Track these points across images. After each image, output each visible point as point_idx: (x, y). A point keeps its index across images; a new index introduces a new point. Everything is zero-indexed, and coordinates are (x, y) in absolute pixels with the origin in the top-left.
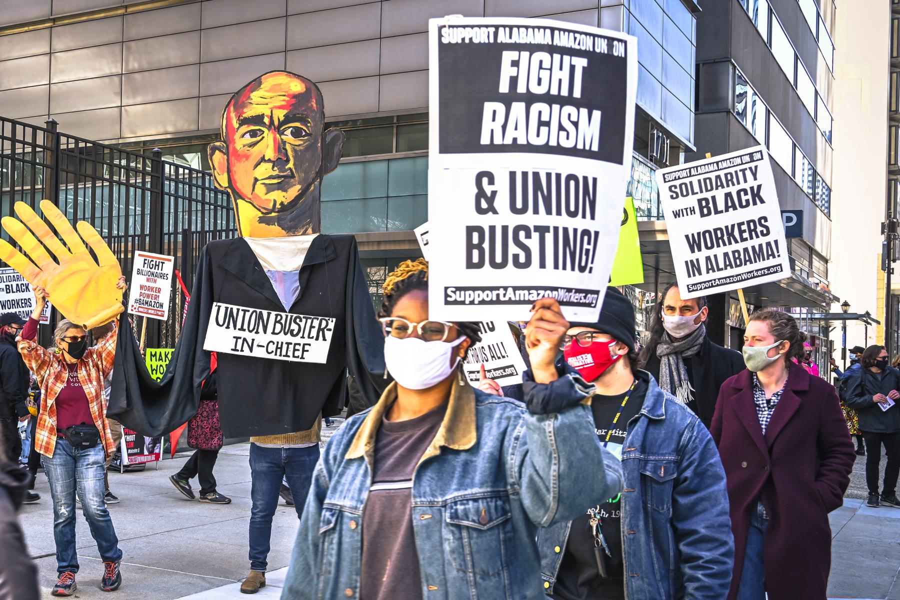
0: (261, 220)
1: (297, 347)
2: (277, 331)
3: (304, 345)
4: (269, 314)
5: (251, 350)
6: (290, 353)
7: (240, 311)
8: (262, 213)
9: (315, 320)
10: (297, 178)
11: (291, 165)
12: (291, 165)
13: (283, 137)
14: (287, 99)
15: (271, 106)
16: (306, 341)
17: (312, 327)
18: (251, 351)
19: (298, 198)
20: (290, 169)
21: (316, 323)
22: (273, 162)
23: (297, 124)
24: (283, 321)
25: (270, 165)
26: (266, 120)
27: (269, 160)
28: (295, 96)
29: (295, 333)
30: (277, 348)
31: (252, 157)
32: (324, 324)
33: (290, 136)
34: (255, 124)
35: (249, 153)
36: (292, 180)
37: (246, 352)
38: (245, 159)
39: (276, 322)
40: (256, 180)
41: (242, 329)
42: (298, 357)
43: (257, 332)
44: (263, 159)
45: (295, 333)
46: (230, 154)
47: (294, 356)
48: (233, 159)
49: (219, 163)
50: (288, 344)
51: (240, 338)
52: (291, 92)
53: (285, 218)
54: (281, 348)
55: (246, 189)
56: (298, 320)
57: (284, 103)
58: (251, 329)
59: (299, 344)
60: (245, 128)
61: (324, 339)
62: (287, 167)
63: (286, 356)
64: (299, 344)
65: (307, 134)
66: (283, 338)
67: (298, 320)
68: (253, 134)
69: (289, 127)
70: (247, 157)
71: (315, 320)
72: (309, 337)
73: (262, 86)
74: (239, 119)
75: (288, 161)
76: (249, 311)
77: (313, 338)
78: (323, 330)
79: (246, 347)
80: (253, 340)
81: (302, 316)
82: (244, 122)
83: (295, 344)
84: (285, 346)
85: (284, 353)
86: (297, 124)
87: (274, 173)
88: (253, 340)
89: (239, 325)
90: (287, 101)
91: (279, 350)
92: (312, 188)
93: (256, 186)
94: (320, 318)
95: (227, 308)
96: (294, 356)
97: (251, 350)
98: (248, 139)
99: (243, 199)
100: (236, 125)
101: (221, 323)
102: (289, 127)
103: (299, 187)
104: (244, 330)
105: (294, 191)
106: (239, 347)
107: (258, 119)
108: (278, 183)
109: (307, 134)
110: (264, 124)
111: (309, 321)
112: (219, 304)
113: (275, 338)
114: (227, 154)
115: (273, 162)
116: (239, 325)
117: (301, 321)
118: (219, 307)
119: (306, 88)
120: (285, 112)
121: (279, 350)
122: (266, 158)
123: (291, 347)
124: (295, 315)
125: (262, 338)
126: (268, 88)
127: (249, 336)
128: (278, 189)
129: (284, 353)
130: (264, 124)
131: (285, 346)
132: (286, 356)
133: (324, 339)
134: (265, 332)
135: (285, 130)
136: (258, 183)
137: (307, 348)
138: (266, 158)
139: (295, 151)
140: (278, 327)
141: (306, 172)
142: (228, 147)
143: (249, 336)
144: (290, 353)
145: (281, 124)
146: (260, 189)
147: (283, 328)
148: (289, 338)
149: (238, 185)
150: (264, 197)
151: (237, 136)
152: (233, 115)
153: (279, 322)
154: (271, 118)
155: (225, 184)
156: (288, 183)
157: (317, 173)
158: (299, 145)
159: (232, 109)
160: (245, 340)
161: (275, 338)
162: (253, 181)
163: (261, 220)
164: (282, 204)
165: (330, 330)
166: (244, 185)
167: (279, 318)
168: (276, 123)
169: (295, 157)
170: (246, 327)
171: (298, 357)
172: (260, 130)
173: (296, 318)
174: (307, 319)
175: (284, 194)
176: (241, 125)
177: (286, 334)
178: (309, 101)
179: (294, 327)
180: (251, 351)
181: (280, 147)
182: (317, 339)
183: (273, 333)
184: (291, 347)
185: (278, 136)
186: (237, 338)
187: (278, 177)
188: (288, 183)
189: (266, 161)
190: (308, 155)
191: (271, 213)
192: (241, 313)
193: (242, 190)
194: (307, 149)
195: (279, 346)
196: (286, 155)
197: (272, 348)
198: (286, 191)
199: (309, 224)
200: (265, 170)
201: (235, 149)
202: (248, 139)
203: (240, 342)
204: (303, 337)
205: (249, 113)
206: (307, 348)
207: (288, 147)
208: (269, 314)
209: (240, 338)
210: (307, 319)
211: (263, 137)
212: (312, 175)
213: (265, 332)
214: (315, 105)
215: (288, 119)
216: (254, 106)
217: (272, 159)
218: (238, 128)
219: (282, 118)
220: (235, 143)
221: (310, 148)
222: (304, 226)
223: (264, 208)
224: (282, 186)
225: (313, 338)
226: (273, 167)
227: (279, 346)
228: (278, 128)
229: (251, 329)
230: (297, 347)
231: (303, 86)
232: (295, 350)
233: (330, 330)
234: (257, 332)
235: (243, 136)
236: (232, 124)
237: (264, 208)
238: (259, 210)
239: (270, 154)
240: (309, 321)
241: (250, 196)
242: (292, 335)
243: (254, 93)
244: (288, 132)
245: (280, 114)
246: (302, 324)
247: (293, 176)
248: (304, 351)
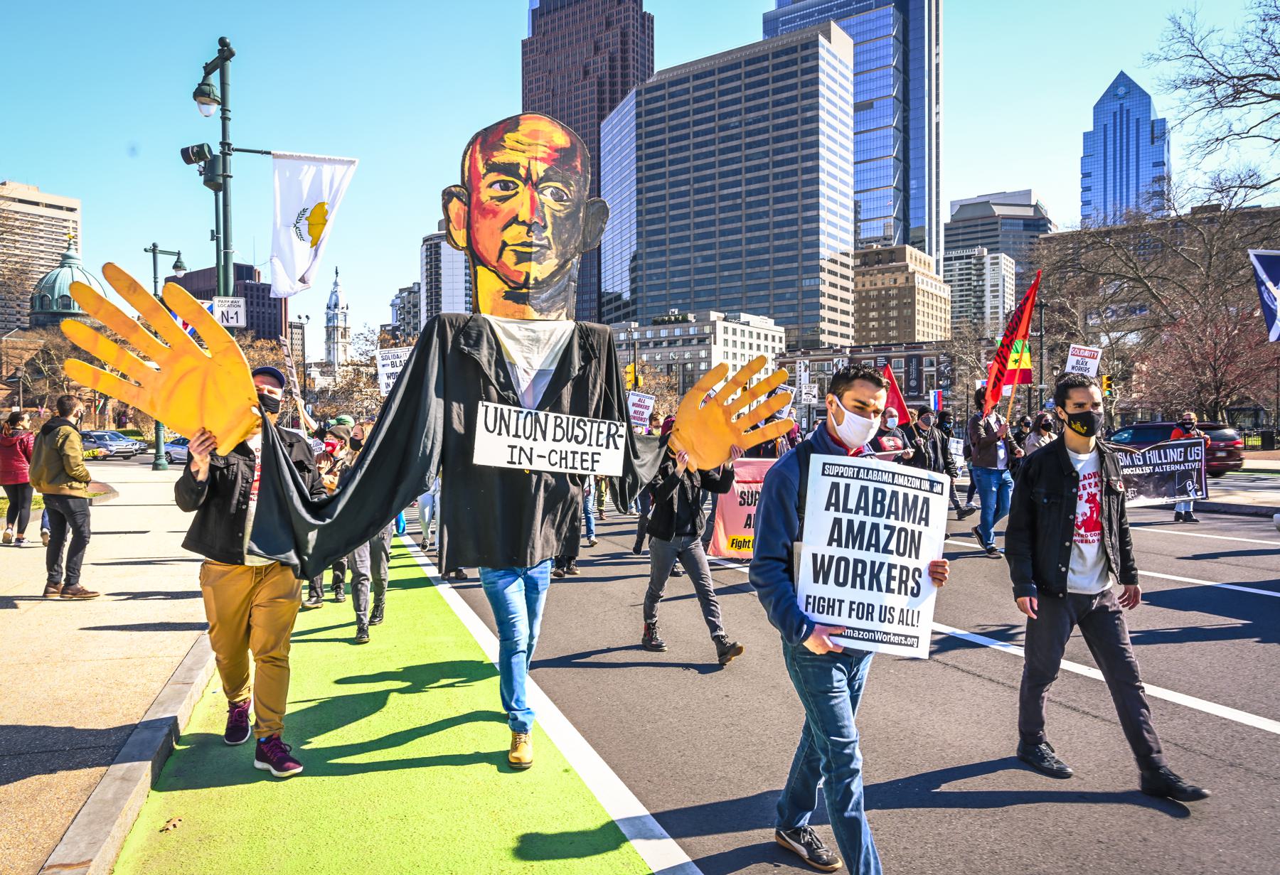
0: (507, 296)
1: (585, 457)
2: (558, 437)
3: (593, 454)
4: (547, 416)
5: (530, 461)
6: (578, 464)
7: (512, 412)
8: (510, 287)
9: (602, 425)
11: (548, 233)
12: (548, 233)
13: (541, 196)
14: (548, 151)
16: (595, 449)
17: (599, 433)
18: (531, 463)
19: (553, 275)
20: (547, 238)
21: (604, 428)
23: (559, 185)
24: (564, 425)
25: (524, 229)
26: (522, 172)
27: (524, 223)
28: (556, 150)
29: (580, 439)
30: (561, 459)
31: (501, 216)
32: (613, 430)
33: (550, 198)
34: (507, 175)
35: (497, 209)
36: (549, 252)
37: (525, 465)
38: (491, 215)
39: (556, 426)
41: (516, 436)
42: (587, 469)
43: (535, 439)
44: (515, 220)
45: (580, 439)
46: (472, 206)
47: (583, 468)
48: (476, 214)
49: (458, 215)
50: (574, 453)
51: (515, 447)
52: (553, 144)
53: (539, 298)
54: (566, 458)
55: (490, 253)
56: (582, 424)
57: (544, 155)
58: (527, 435)
59: (587, 454)
60: (493, 177)
61: (616, 448)
62: (544, 235)
63: (573, 468)
64: (587, 454)
66: (566, 446)
67: (582, 424)
68: (505, 185)
69: (549, 187)
70: (495, 213)
71: (602, 425)
72: (597, 445)
73: (520, 128)
74: (486, 164)
75: (545, 227)
76: (522, 412)
77: (602, 445)
78: (613, 436)
79: (524, 459)
80: (532, 449)
81: (586, 419)
82: (492, 168)
83: (582, 453)
84: (570, 456)
85: (570, 464)
86: (559, 185)
88: (532, 449)
89: (512, 431)
90: (549, 155)
91: (563, 461)
93: (505, 253)
94: (608, 422)
95: (496, 409)
96: (583, 468)
97: (530, 461)
98: (497, 191)
99: (486, 266)
100: (482, 170)
101: (491, 429)
102: (549, 187)
103: (556, 261)
104: (520, 437)
106: (516, 459)
107: (511, 169)
110: (519, 177)
111: (595, 425)
112: (486, 403)
113: (557, 446)
116: (512, 431)
117: (585, 425)
118: (487, 407)
119: (571, 143)
120: (546, 166)
121: (563, 461)
122: (520, 219)
123: (578, 457)
124: (577, 418)
125: (542, 447)
126: (526, 132)
127: (527, 445)
129: (570, 464)
130: (519, 177)
131: (570, 456)
132: (573, 468)
133: (616, 448)
134: (544, 439)
135: (544, 188)
136: (507, 248)
137: (596, 457)
138: (520, 219)
139: (554, 216)
140: (559, 431)
141: (565, 245)
142: (470, 196)
143: (527, 445)
144: (578, 464)
146: (509, 258)
147: (565, 434)
148: (573, 446)
149: (480, 247)
150: (513, 268)
151: (483, 184)
152: (479, 156)
153: (560, 426)
154: (528, 170)
158: (559, 211)
159: (478, 148)
160: (521, 449)
161: (557, 446)
162: (500, 245)
163: (507, 296)
164: (536, 279)
165: (621, 436)
167: (559, 421)
168: (534, 178)
169: (554, 224)
170: (521, 432)
171: (587, 469)
172: (513, 182)
173: (579, 421)
174: (592, 422)
176: (489, 171)
177: (569, 441)
178: (573, 158)
179: (578, 432)
180: (531, 463)
182: (608, 447)
183: (554, 440)
184: (578, 457)
186: (513, 447)
188: (544, 255)
191: (521, 288)
192: (514, 416)
193: (485, 254)
194: (568, 217)
195: (564, 456)
196: (543, 219)
197: (555, 458)
199: (563, 308)
202: (497, 191)
203: (516, 451)
204: (590, 445)
205: (500, 157)
206: (596, 457)
208: (547, 416)
209: (515, 447)
210: (592, 422)
211: (517, 193)
213: (544, 439)
214: (579, 167)
216: (507, 150)
217: (527, 221)
218: (485, 175)
219: (542, 174)
220: (479, 192)
221: (572, 216)
222: (558, 309)
223: (513, 281)
225: (602, 445)
227: (564, 456)
229: (527, 435)
230: (585, 457)
231: (568, 139)
232: (583, 461)
233: (621, 436)
234: (535, 439)
235: (491, 186)
236: (476, 168)
237: (513, 281)
238: (506, 283)
240: (595, 425)
241: (496, 264)
242: (578, 442)
243: (509, 135)
244: (548, 192)
246: (588, 429)
247: (549, 248)
248: (593, 461)
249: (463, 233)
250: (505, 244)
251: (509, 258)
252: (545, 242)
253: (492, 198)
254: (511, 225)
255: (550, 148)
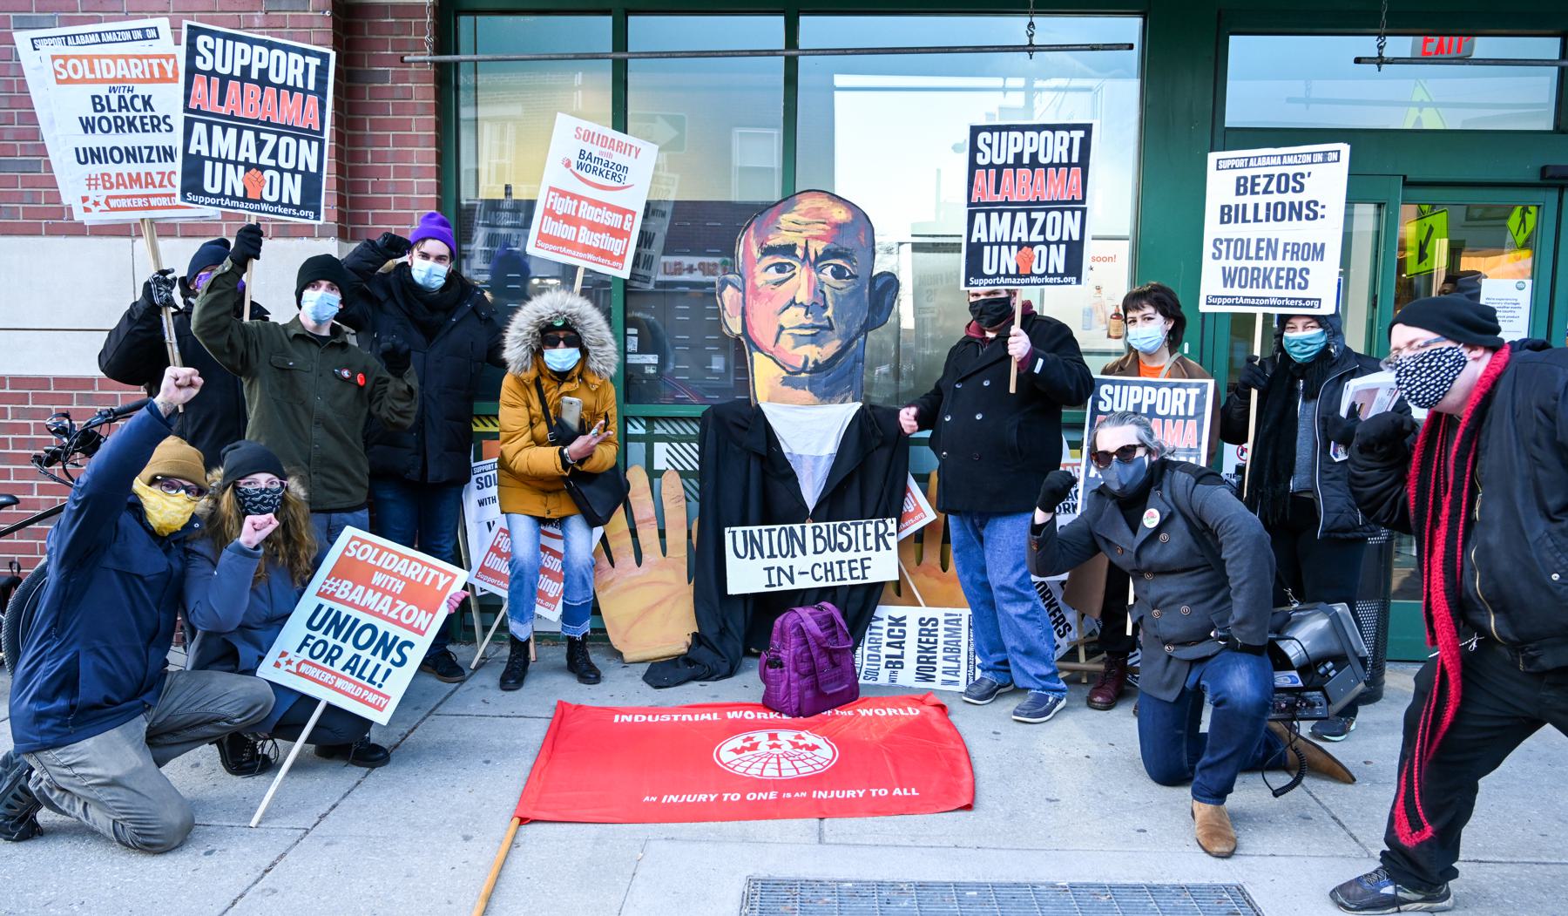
10: (836, 331)
11: (829, 313)
13: (821, 276)
14: (828, 228)
15: (805, 234)
20: (828, 318)
22: (807, 307)
23: (839, 262)
26: (799, 252)
33: (830, 275)
34: (785, 255)
35: (773, 292)
40: (782, 328)
52: (833, 220)
60: (769, 260)
65: (852, 276)
68: (781, 268)
75: (825, 307)
82: (768, 251)
87: (808, 322)
92: (854, 346)
99: (761, 352)
103: (838, 342)
105: (831, 348)
107: (789, 250)
108: (812, 335)
109: (852, 276)
114: (744, 291)
115: (807, 307)
126: (803, 212)
128: (812, 343)
138: (797, 301)
145: (818, 259)
151: (759, 268)
152: (753, 241)
154: (806, 249)
155: (737, 330)
156: (824, 336)
157: (862, 327)
159: (752, 232)
162: (777, 329)
166: (763, 331)
168: (812, 257)
172: (790, 264)
175: (819, 349)
181: (818, 291)
185: (814, 274)
187: (813, 327)
189: (796, 304)
190: (852, 302)
198: (821, 346)
200: (795, 317)
201: (754, 285)
205: (775, 241)
207: (826, 289)
211: (794, 274)
212: (856, 328)
215: (829, 254)
217: (806, 303)
218: (759, 260)
220: (754, 277)
224: (815, 339)
226: (806, 314)
228: (817, 263)
235: (766, 270)
236: (751, 253)
239: (803, 296)
241: (773, 350)
243: (785, 216)
245: (818, 247)
247: (831, 328)
249: (739, 319)
250: (782, 328)
251: (786, 341)
252: (826, 323)
253: (767, 283)
254: (787, 308)
255: (830, 224)
